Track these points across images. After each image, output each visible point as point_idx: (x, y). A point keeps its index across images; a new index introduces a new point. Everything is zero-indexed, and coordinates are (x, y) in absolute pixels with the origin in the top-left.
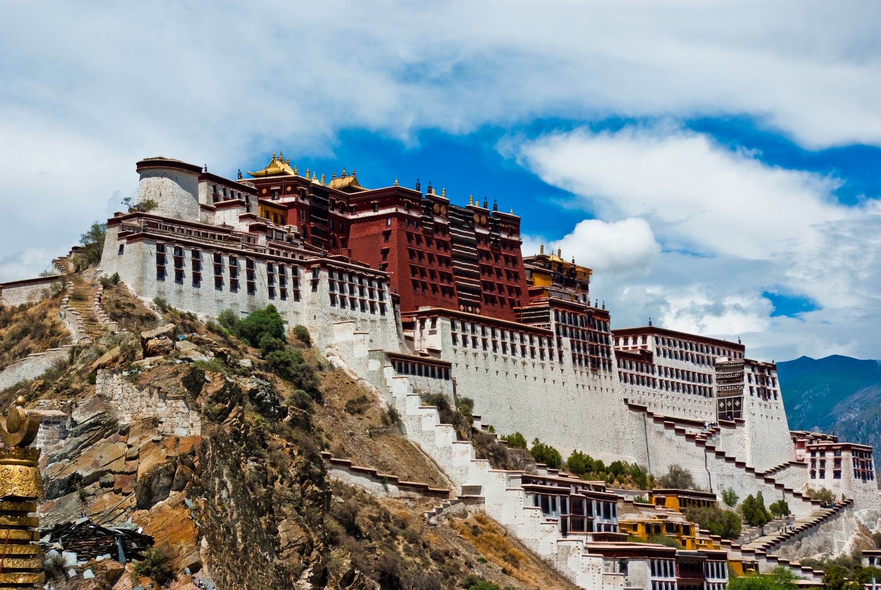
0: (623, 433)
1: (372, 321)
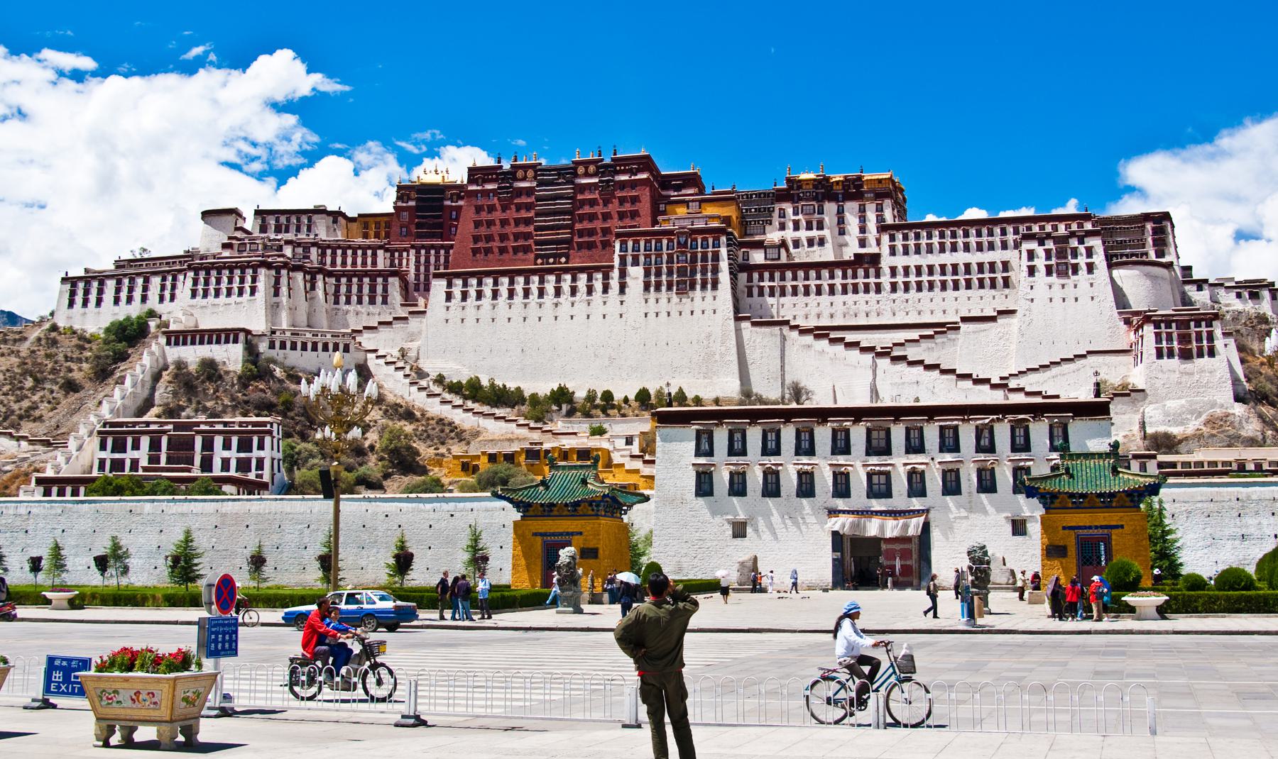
0: (721, 354)
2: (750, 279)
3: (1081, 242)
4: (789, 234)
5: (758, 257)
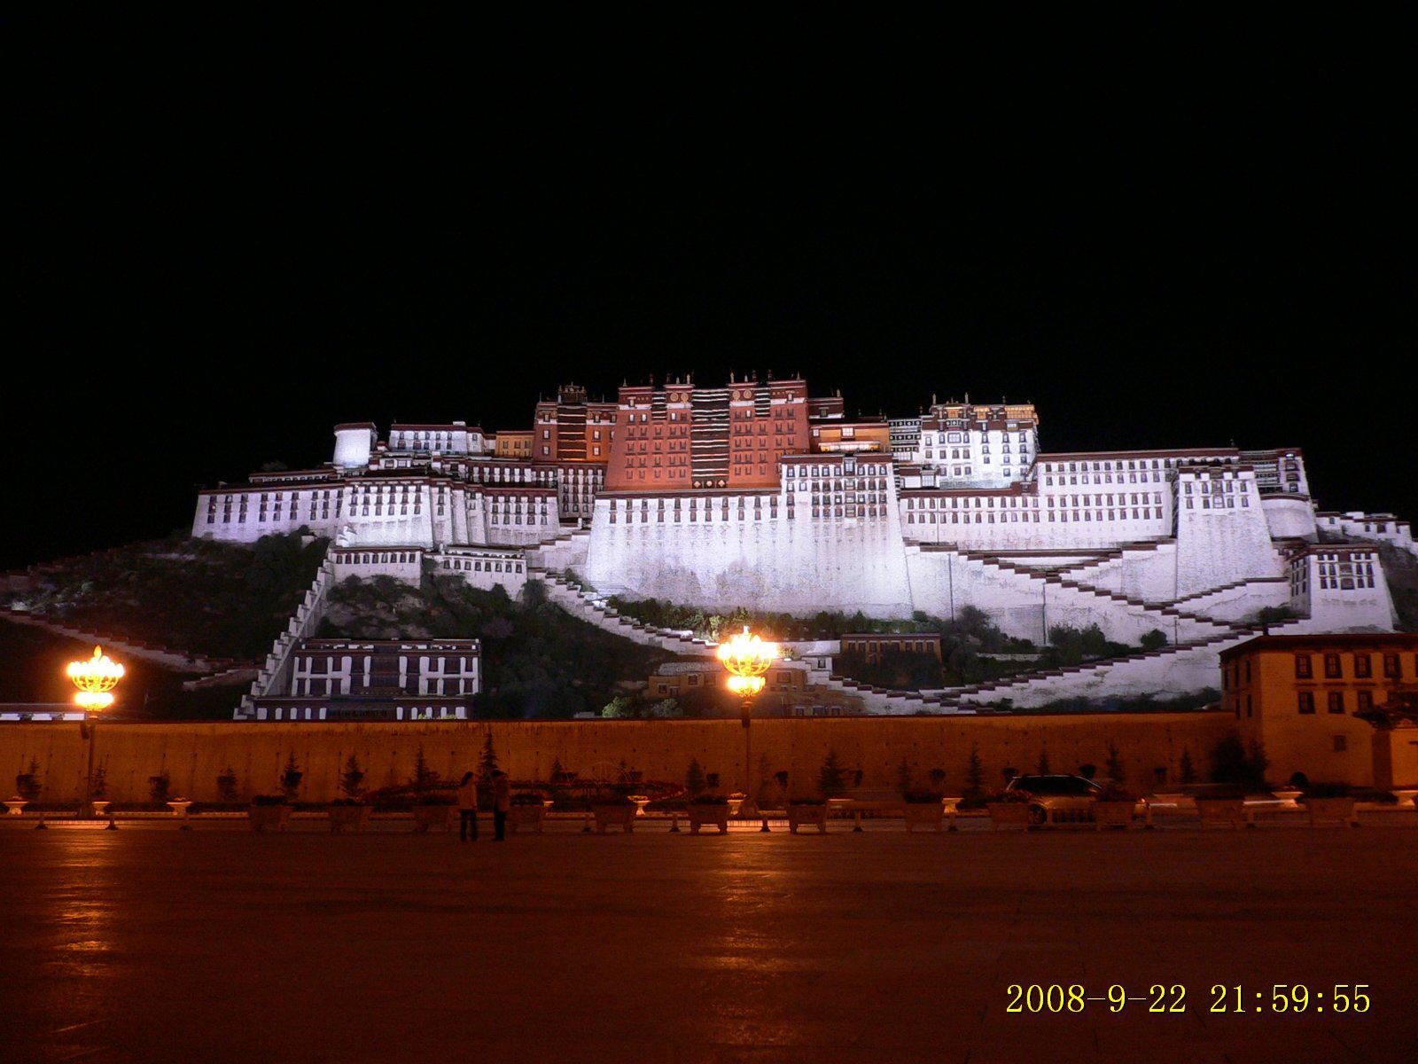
1: (401, 522)
2: (911, 506)
3: (1236, 476)
4: (936, 459)
5: (912, 482)
